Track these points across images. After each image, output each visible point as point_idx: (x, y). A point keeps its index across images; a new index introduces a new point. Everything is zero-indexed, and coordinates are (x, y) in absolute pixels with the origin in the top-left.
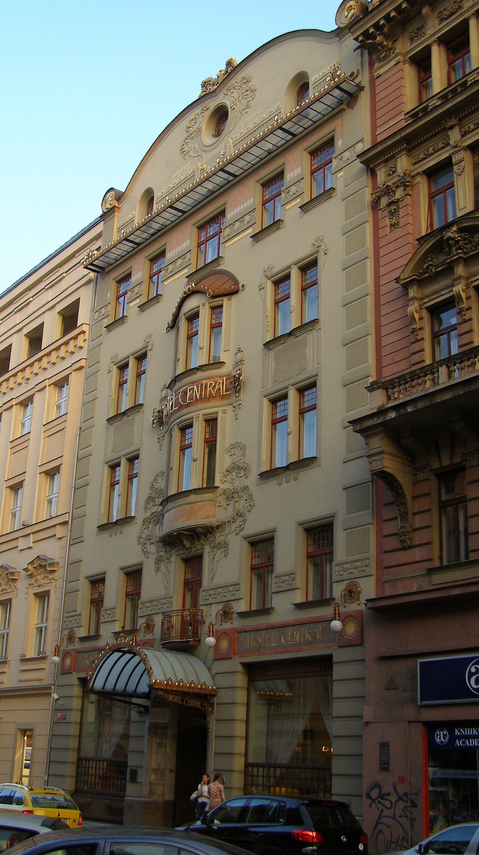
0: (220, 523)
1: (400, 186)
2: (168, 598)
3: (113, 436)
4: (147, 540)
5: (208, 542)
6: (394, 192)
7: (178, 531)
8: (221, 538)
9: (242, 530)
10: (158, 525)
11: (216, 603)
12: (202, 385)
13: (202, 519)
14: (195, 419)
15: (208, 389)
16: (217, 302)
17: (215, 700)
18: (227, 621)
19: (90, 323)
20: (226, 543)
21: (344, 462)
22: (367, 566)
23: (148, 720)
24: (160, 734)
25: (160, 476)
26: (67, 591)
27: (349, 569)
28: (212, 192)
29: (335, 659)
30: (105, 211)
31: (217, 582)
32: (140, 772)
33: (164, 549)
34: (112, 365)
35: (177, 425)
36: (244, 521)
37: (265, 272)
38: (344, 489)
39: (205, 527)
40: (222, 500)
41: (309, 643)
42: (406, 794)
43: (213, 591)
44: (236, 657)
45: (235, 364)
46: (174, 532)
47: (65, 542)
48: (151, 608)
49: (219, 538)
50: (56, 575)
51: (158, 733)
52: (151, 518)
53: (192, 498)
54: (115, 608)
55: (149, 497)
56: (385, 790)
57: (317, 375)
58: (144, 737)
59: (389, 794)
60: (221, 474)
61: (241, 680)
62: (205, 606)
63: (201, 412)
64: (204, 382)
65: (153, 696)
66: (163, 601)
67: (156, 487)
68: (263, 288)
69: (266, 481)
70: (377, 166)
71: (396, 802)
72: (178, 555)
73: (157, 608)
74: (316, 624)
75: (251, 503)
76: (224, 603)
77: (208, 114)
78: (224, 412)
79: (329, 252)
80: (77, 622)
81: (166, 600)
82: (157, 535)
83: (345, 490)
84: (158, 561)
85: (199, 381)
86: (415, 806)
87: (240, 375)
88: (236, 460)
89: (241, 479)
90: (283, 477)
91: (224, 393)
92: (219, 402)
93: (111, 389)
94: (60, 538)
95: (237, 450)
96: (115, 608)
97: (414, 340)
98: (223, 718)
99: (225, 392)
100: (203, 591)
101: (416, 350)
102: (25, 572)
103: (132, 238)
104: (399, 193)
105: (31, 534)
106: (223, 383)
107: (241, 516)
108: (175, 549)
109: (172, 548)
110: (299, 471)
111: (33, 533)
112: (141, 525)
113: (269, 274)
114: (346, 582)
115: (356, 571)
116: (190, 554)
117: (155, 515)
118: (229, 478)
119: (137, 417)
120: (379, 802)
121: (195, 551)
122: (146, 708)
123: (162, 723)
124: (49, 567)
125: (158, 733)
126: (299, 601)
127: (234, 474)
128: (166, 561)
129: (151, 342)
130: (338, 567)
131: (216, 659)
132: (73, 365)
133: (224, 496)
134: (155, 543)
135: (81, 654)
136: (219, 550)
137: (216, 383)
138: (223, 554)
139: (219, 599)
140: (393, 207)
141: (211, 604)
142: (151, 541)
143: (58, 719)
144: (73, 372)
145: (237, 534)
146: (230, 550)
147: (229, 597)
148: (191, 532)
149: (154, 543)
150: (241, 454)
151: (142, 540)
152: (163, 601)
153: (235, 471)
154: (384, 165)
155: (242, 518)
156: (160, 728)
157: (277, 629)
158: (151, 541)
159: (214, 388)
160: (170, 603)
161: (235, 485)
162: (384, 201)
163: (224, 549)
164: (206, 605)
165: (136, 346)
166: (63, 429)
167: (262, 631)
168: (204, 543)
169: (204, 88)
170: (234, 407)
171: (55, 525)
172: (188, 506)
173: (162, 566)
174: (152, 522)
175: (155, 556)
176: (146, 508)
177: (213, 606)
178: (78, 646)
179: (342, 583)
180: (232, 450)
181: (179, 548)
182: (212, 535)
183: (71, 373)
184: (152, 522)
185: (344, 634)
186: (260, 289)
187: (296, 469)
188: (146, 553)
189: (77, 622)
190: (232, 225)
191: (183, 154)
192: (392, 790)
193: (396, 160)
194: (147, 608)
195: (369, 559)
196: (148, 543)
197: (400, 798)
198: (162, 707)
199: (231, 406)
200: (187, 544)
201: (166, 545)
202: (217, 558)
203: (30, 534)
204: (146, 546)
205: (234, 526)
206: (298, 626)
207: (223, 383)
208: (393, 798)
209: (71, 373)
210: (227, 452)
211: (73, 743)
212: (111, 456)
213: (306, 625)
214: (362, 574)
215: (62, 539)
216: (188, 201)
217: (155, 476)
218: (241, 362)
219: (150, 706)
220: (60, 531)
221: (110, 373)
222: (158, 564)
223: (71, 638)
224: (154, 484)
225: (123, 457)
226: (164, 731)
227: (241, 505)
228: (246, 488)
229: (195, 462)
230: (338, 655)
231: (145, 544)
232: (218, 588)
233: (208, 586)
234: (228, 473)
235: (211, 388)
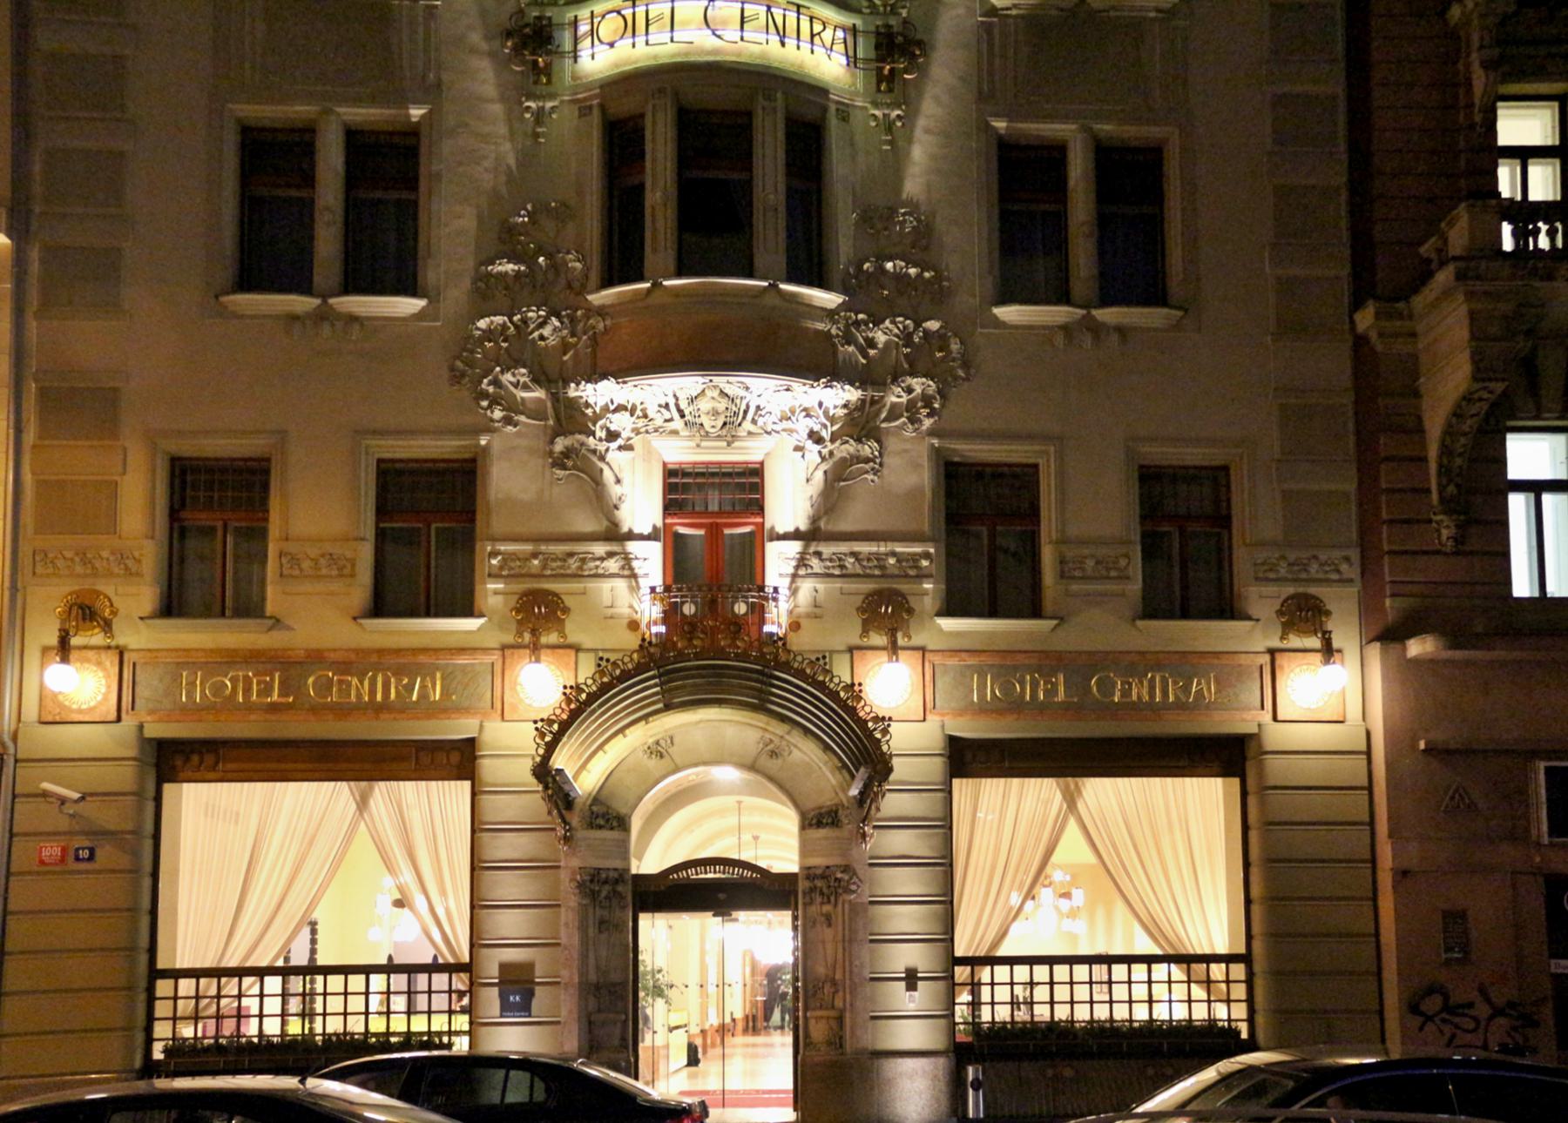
24: (606, 898)
42: (1511, 1005)
51: (604, 894)
56: (1457, 997)
59: (1471, 1005)
71: (1491, 1018)
86: (1536, 1024)
120: (1444, 1021)
123: (616, 870)
125: (604, 894)
156: (606, 882)
192: (1474, 995)
197: (1498, 1012)
198: (612, 829)
208: (1482, 1010)
226: (620, 888)
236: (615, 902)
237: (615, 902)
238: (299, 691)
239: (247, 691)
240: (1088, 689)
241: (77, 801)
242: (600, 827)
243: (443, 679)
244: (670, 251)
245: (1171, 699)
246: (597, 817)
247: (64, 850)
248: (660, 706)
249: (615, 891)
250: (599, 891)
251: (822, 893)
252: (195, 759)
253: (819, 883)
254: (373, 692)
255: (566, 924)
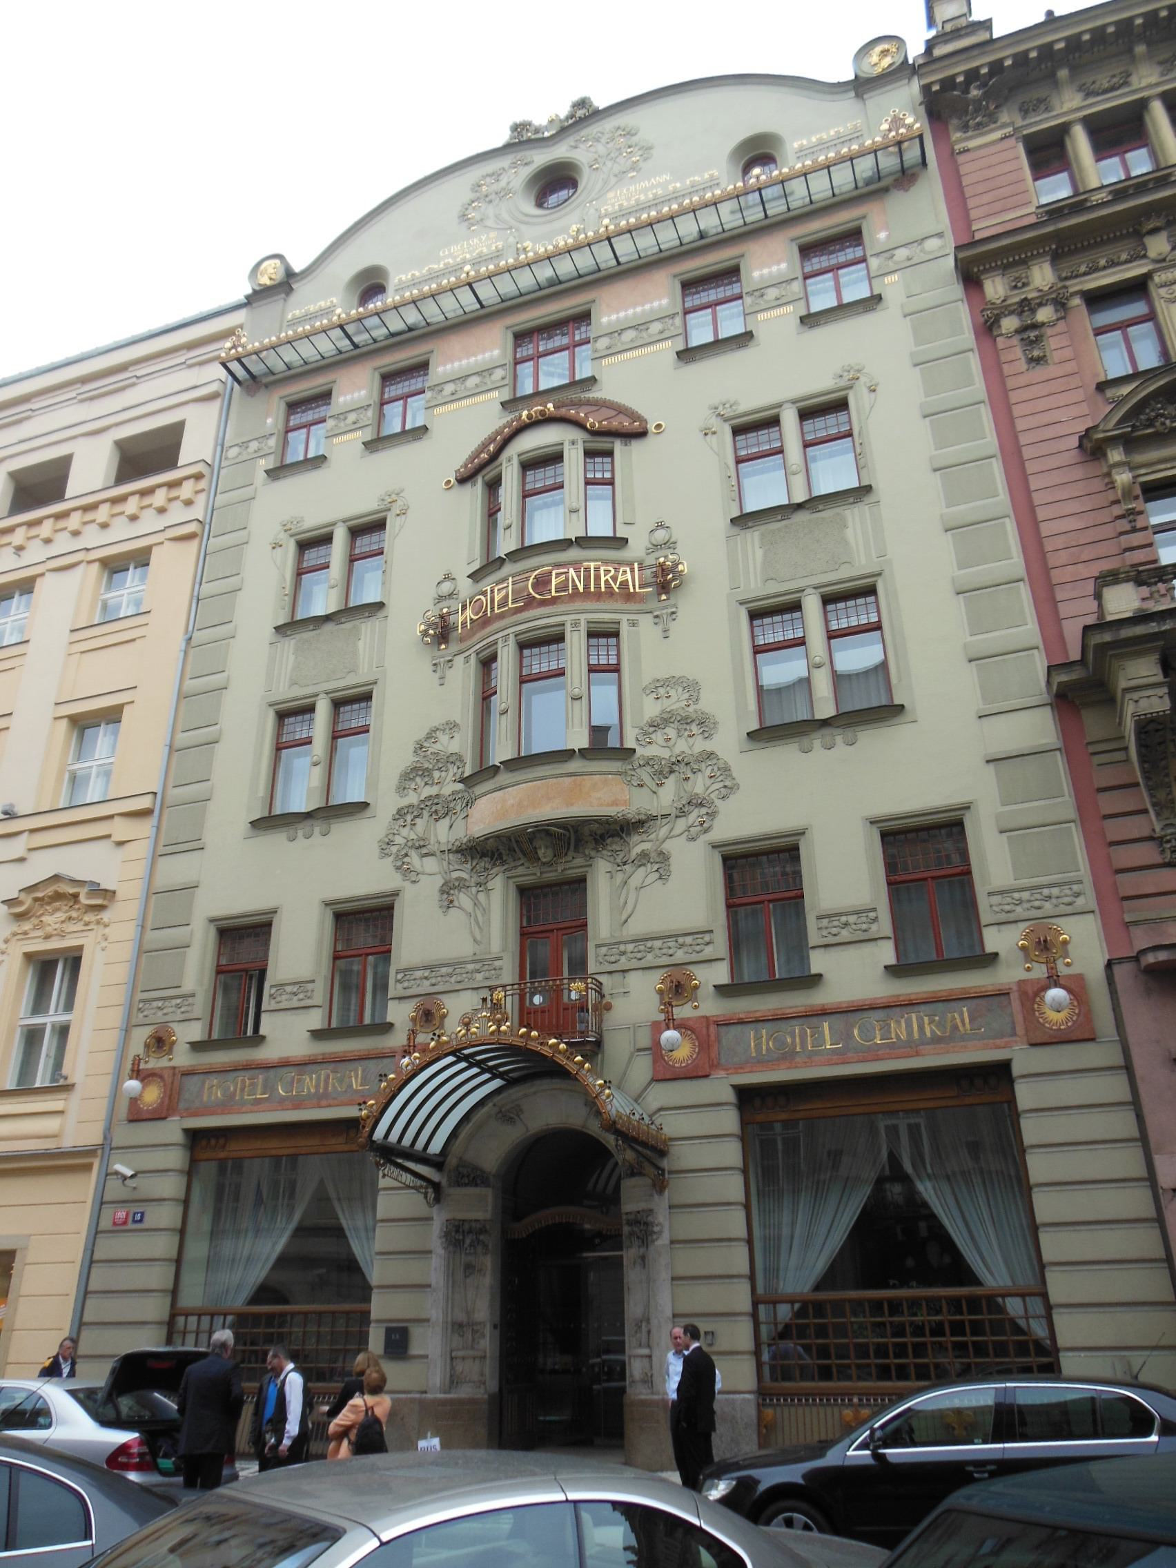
0: (643, 817)
1: (1046, 305)
2: (483, 962)
3: (292, 658)
4: (412, 847)
5: (604, 852)
6: (1033, 311)
7: (536, 826)
8: (646, 846)
9: (706, 831)
10: (446, 822)
11: (643, 969)
12: (587, 570)
13: (602, 805)
14: (568, 628)
15: (603, 579)
16: (601, 444)
17: (665, 1164)
18: (680, 1003)
19: (214, 461)
20: (661, 853)
21: (980, 717)
22: (1077, 895)
23: (439, 1218)
24: (471, 1245)
25: (444, 730)
26: (146, 947)
27: (1029, 901)
28: (555, 281)
29: (1016, 1070)
30: (257, 288)
31: (636, 927)
32: (416, 1332)
33: (469, 866)
34: (283, 536)
35: (516, 636)
36: (712, 815)
37: (716, 408)
38: (988, 762)
39: (607, 822)
40: (645, 774)
41: (936, 1040)
43: (633, 945)
44: (722, 1074)
45: (650, 546)
46: (531, 827)
47: (141, 850)
48: (433, 981)
49: (639, 845)
50: (106, 916)
51: (468, 1241)
52: (422, 806)
53: (575, 765)
54: (313, 981)
55: (415, 769)
57: (880, 574)
58: (430, 1252)
60: (637, 731)
61: (729, 1120)
62: (606, 975)
63: (583, 618)
64: (592, 565)
65: (452, 1161)
66: (470, 967)
67: (431, 750)
68: (714, 433)
69: (767, 745)
70: (986, 271)
72: (508, 878)
73: (453, 980)
74: (953, 1004)
75: (728, 783)
76: (666, 969)
77: (526, 172)
78: (633, 624)
79: (878, 389)
80: (183, 1010)
81: (481, 964)
82: (443, 839)
83: (991, 765)
84: (448, 890)
85: (581, 562)
87: (676, 564)
88: (672, 708)
89: (691, 740)
90: (817, 740)
91: (637, 590)
92: (620, 605)
93: (283, 577)
94: (120, 844)
95: (674, 691)
96: (313, 981)
97: (1128, 527)
98: (689, 1201)
99: (640, 588)
100: (598, 946)
101: (1135, 544)
102: (6, 907)
103: (350, 329)
104: (1044, 314)
105: (26, 834)
106: (632, 570)
107: (701, 805)
108: (502, 864)
109: (494, 865)
110: (857, 729)
111: (32, 831)
112: (390, 818)
113: (728, 412)
114: (1022, 926)
115: (1048, 905)
116: (544, 875)
117: (436, 801)
118: (658, 737)
119: (367, 628)
121: (565, 869)
122: (436, 1186)
124: (88, 898)
125: (468, 1241)
126: (892, 960)
127: (671, 732)
128: (474, 890)
129: (399, 503)
130: (996, 899)
131: (655, 1080)
132: (167, 530)
133: (648, 769)
134: (438, 853)
135: (196, 1078)
136: (642, 868)
137: (616, 570)
138: (657, 875)
139: (650, 959)
140: (1032, 334)
141: (624, 971)
142: (424, 851)
143: (115, 1224)
144: (166, 542)
145: (693, 839)
146: (672, 868)
147: (680, 956)
148: (565, 828)
149: (432, 855)
150: (686, 696)
151: (394, 849)
152: (470, 967)
153: (672, 725)
154: (1001, 272)
155: (704, 811)
156: (470, 1231)
157: (838, 1015)
158: (424, 851)
159: (615, 578)
160: (495, 969)
161: (677, 750)
162: (1009, 324)
163: (656, 867)
164: (610, 973)
165: (362, 505)
166: (134, 640)
167: (794, 1022)
168: (593, 853)
169: (516, 134)
170: (657, 617)
171: (111, 817)
172: (568, 780)
173: (463, 899)
174: (426, 814)
175: (439, 881)
176: (404, 788)
177: (632, 974)
178: (182, 1058)
179: (1013, 926)
180: (662, 691)
181: (513, 864)
182: (616, 839)
183: (162, 543)
184: (426, 814)
185: (1041, 1020)
186: (706, 434)
187: (848, 725)
188: (405, 870)
189: (183, 1010)
190: (616, 334)
191: (466, 223)
193: (1028, 268)
194: (418, 982)
195: (1080, 882)
196: (413, 853)
198: (476, 1185)
199: (650, 616)
200: (544, 853)
201: (472, 858)
202: (636, 880)
203: (25, 831)
204: (406, 859)
205: (681, 824)
206: (898, 1009)
207: (632, 570)
209: (162, 543)
210: (648, 692)
211: (160, 1277)
212: (286, 692)
213: (923, 1007)
214: (1069, 909)
215: (127, 846)
216: (506, 286)
217: (427, 730)
218: (669, 544)
219: (444, 1182)
220: (121, 829)
221: (279, 550)
222: (448, 893)
223: (160, 1042)
224: (425, 744)
225: (323, 696)
226: (482, 1237)
227: (699, 785)
228: (710, 755)
229: (578, 702)
230: (1023, 1060)
231: (406, 855)
232: (647, 940)
233: (612, 936)
234: (653, 729)
235: (608, 577)
236: (479, 1249)
237: (479, 1249)
238: (273, 1090)
239: (243, 1090)
240: (850, 1036)
241: (132, 1176)
242: (466, 1185)
243: (363, 1071)
244: (510, 742)
245: (928, 1034)
246: (463, 1176)
247: (127, 1215)
248: (497, 1083)
249: (479, 1241)
250: (464, 1241)
251: (638, 1237)
252: (213, 1142)
253: (636, 1229)
254: (317, 1086)
255: (435, 1269)
